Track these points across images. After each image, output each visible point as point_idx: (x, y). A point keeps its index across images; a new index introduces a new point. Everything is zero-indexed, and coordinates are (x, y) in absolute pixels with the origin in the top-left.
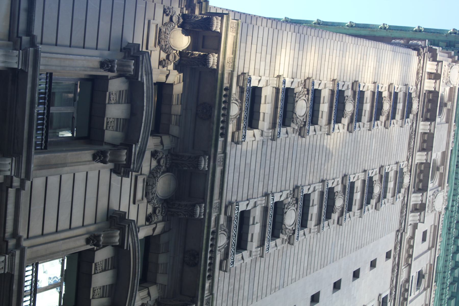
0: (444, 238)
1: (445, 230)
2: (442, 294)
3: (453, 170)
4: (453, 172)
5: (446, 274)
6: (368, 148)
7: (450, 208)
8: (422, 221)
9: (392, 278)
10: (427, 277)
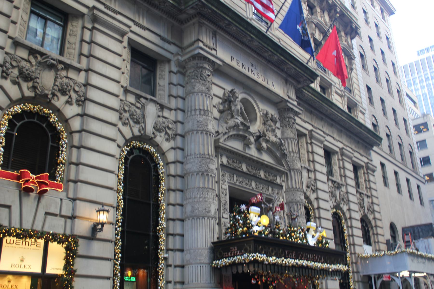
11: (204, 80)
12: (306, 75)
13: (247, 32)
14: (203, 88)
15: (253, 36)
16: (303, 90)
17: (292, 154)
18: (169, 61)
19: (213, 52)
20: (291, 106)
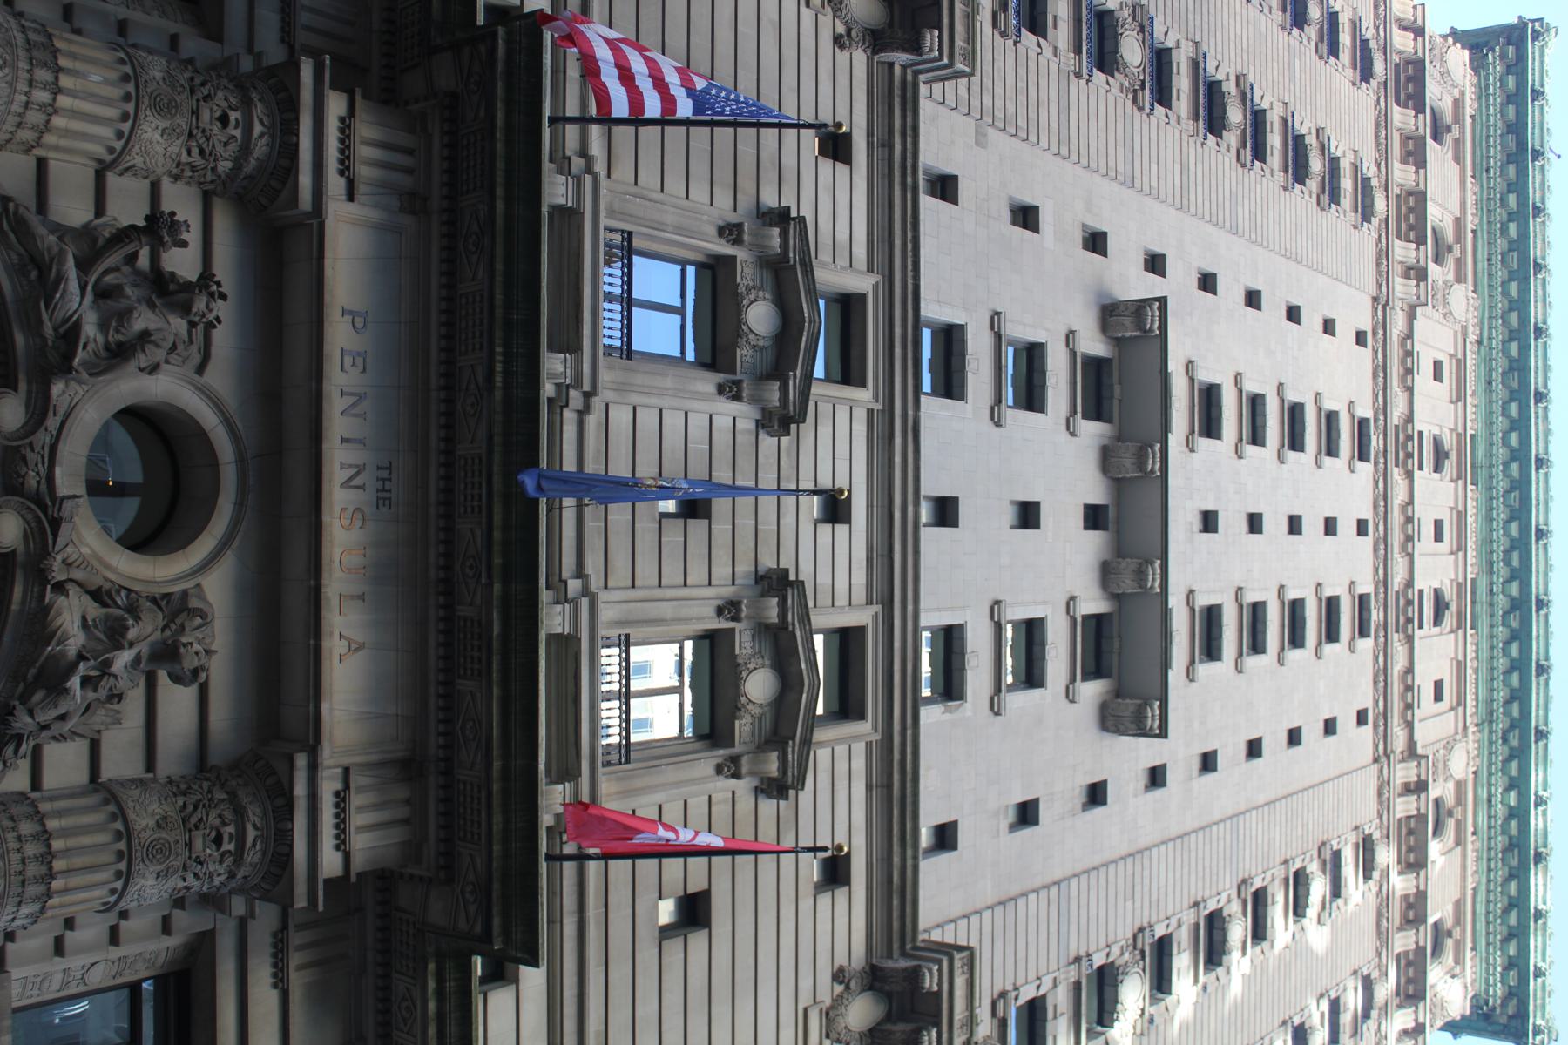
0: (1481, 399)
1: (1483, 386)
2: (1491, 509)
3: (1483, 270)
4: (1483, 272)
5: (1494, 470)
6: (1286, 66)
7: (1485, 342)
8: (1423, 299)
9: (1374, 390)
10: (1453, 456)
11: (192, 92)
12: (496, 848)
13: (498, 334)
14: (158, 75)
15: (499, 378)
16: (432, 967)
17: (27, 828)
18: (215, 34)
19: (335, 183)
20: (300, 790)
